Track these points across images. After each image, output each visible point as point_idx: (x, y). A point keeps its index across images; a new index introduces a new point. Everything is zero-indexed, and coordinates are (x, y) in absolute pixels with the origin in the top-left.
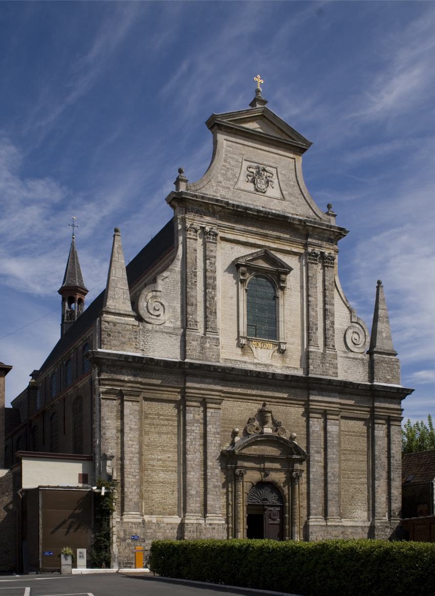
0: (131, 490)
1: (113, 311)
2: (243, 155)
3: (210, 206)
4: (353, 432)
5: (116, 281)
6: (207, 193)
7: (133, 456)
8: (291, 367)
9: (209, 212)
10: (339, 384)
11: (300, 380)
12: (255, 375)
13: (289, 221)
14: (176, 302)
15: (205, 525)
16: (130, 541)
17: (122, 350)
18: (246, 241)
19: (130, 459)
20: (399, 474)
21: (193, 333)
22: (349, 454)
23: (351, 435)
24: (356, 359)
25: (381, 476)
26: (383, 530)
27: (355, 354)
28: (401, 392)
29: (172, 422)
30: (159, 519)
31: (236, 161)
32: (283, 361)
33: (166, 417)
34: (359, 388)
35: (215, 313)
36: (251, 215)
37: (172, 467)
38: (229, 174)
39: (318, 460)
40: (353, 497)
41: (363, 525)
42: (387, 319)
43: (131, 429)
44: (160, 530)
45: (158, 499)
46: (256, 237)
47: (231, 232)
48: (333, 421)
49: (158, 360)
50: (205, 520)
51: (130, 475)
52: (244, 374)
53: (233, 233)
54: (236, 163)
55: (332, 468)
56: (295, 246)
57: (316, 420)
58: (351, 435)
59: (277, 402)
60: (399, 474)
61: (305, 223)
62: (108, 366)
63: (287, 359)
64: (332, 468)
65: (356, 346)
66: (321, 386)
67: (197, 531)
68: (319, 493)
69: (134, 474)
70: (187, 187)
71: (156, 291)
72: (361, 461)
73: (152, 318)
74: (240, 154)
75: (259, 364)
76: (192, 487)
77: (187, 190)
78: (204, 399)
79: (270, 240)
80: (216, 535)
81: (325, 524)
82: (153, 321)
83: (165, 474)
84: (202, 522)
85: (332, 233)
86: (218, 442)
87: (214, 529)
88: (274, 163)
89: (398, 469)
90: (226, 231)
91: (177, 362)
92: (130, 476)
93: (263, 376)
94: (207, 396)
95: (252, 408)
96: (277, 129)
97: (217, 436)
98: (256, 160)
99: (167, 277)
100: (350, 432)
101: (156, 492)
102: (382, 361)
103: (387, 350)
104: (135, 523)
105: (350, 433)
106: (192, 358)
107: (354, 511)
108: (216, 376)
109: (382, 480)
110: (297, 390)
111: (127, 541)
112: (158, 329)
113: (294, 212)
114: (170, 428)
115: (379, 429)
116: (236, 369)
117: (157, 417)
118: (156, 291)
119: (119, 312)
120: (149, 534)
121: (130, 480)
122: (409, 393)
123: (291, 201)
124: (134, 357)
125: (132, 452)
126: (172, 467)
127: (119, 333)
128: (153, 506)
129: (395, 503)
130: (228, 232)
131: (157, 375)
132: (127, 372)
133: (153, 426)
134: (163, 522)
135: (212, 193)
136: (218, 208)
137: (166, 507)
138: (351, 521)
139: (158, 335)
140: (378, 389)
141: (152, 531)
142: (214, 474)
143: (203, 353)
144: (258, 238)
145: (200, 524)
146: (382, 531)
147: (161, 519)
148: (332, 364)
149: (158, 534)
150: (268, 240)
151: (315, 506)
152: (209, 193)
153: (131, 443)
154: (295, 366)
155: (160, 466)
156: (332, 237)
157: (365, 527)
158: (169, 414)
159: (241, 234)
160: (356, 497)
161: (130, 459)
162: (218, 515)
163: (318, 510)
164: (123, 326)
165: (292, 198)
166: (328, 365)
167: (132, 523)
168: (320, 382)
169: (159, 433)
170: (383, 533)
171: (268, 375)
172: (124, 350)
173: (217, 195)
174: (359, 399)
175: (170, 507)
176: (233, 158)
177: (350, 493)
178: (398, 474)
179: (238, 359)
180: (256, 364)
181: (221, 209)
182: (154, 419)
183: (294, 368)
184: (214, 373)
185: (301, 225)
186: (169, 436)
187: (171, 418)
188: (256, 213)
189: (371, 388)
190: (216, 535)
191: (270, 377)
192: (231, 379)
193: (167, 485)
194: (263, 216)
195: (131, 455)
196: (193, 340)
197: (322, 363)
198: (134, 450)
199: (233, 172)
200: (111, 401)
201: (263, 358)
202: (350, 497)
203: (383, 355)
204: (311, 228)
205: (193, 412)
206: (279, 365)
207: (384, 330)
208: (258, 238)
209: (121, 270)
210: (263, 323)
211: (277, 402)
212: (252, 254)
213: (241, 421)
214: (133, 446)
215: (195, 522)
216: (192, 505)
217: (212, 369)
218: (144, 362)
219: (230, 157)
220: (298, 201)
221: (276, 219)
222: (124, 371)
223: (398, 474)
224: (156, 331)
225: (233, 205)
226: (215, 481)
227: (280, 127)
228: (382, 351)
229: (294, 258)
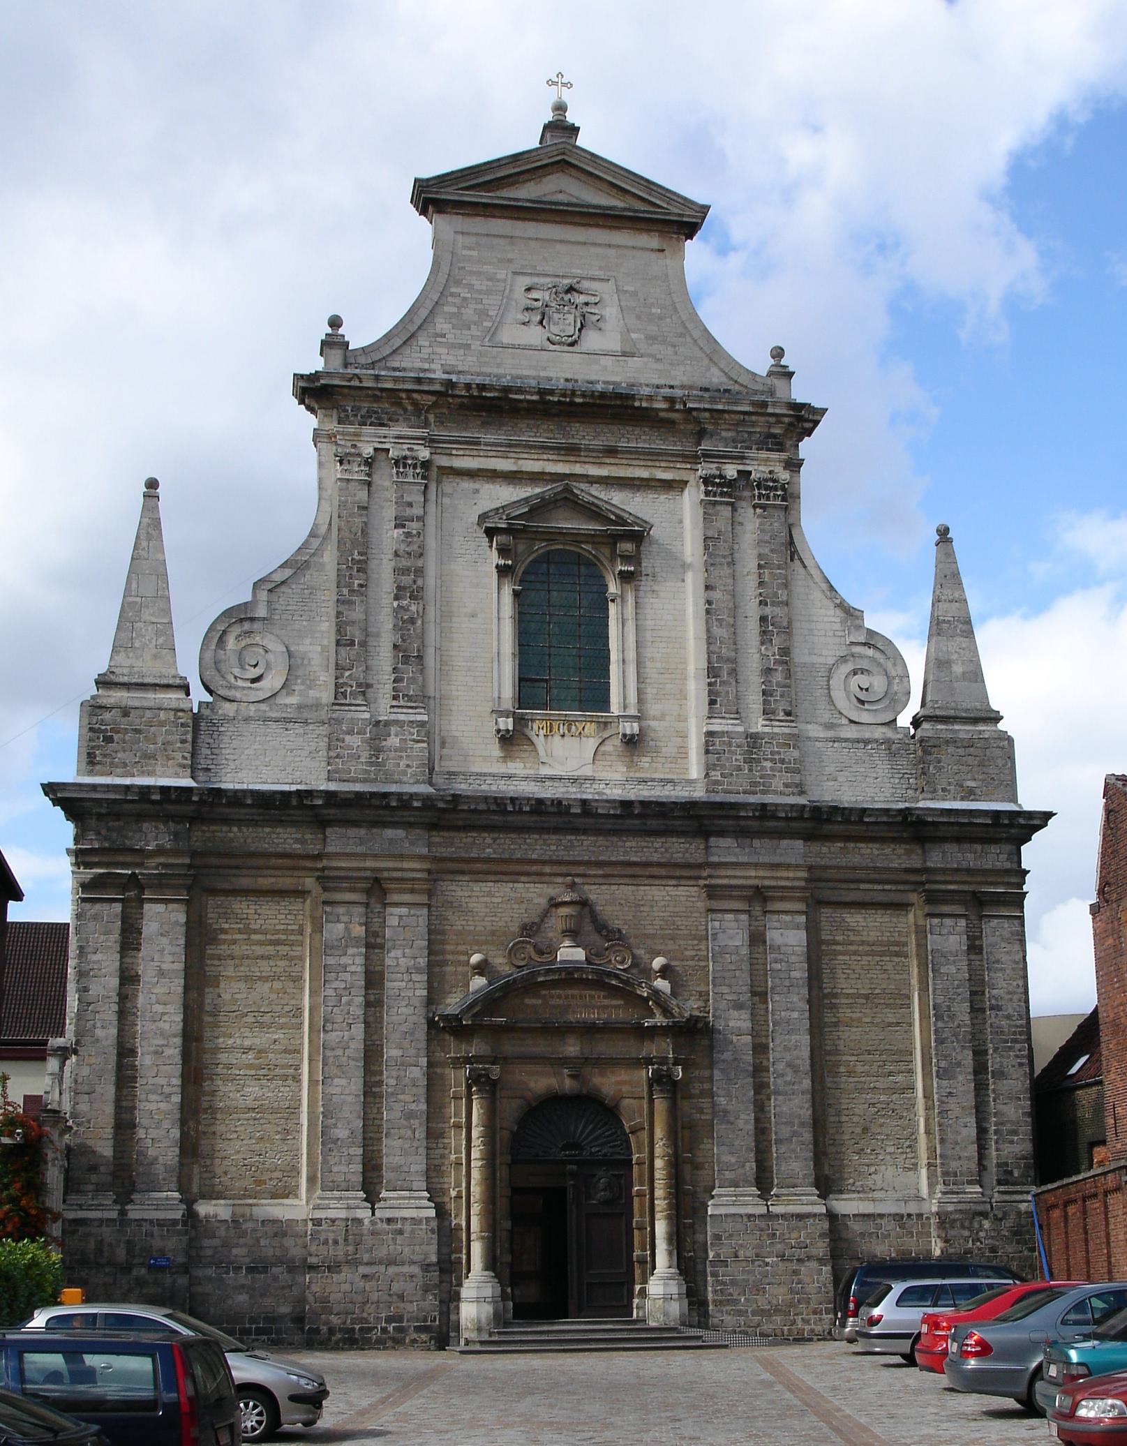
0: (153, 1133)
1: (126, 679)
2: (510, 261)
3: (404, 395)
4: (863, 943)
5: (137, 608)
6: (404, 365)
7: (165, 1042)
8: (653, 780)
9: (405, 410)
10: (794, 815)
11: (672, 810)
12: (528, 809)
13: (637, 404)
14: (308, 641)
15: (373, 1223)
16: (143, 1271)
17: (142, 773)
18: (514, 468)
19: (156, 1053)
20: (1023, 1056)
21: (349, 715)
22: (850, 1006)
23: (855, 953)
24: (866, 742)
25: (959, 1064)
26: (966, 1224)
27: (864, 727)
28: (1006, 822)
29: (287, 948)
30: (239, 1210)
31: (489, 280)
32: (631, 765)
33: (269, 937)
34: (867, 820)
35: (420, 658)
36: (525, 405)
37: (283, 1067)
38: (469, 313)
39: (739, 1029)
40: (865, 1130)
41: (903, 1211)
42: (964, 627)
43: (161, 973)
44: (241, 1241)
45: (240, 1156)
46: (545, 457)
47: (467, 452)
48: (787, 918)
49: (236, 791)
50: (373, 1209)
51: (155, 1093)
52: (493, 807)
53: (474, 453)
54: (490, 283)
55: (787, 1049)
56: (663, 464)
57: (730, 916)
58: (855, 953)
59: (604, 876)
60: (1023, 1056)
61: (685, 405)
62: (100, 816)
63: (644, 759)
64: (787, 1049)
65: (867, 706)
66: (742, 823)
67: (346, 1240)
68: (746, 1122)
69: (167, 1090)
70: (345, 357)
71: (252, 619)
72: (890, 1025)
73: (236, 688)
74: (500, 261)
75: (551, 778)
76: (337, 1119)
77: (346, 365)
78: (377, 880)
79: (587, 460)
80: (406, 1250)
81: (763, 1210)
82: (238, 695)
83: (262, 1087)
84: (364, 1214)
85: (772, 420)
86: (418, 993)
87: (401, 1232)
88: (601, 269)
89: (1015, 1041)
90: (454, 452)
91: (290, 792)
92: (153, 1097)
93: (551, 809)
94: (386, 874)
95: (530, 895)
96: (605, 187)
97: (416, 977)
98: (550, 270)
99: (283, 583)
100: (851, 943)
101: (235, 1136)
102: (947, 742)
103: (967, 710)
104: (160, 1223)
105: (851, 948)
106: (346, 776)
107: (872, 1169)
108: (412, 820)
109: (960, 1078)
110: (674, 840)
111: (135, 1272)
112: (252, 714)
113: (662, 382)
114: (281, 963)
115: (944, 931)
116: (468, 797)
117: (245, 936)
118: (252, 619)
119: (140, 681)
120: (209, 1252)
121: (153, 1107)
122: (1037, 822)
123: (653, 356)
124: (165, 790)
125: (162, 1034)
126: (283, 1067)
127: (138, 731)
128: (226, 1173)
129: (1012, 1142)
130: (461, 452)
131: (245, 830)
132: (157, 828)
133: (232, 962)
134: (251, 1218)
135: (418, 365)
136: (425, 397)
137: (265, 1177)
138: (860, 1199)
139: (253, 726)
140: (930, 819)
141: (216, 1242)
142: (407, 1081)
143: (378, 764)
144: (551, 457)
145: (359, 1221)
146: (963, 1227)
147: (247, 1210)
148: (782, 761)
149: (235, 1251)
150: (582, 459)
151: (733, 1160)
152: (409, 365)
153: (159, 1008)
154: (667, 776)
155: (250, 1066)
156: (776, 430)
157: (909, 1215)
158: (278, 927)
159: (499, 454)
160: (874, 1129)
161: (156, 1053)
162: (416, 1194)
163: (741, 1171)
164: (148, 714)
165: (656, 348)
166: (768, 764)
167: (151, 1221)
168: (732, 813)
169: (247, 979)
170: (966, 1233)
171: (569, 806)
172: (150, 774)
173: (433, 366)
174: (876, 852)
175: (276, 1175)
176: (479, 273)
177: (856, 1119)
178: (1017, 1056)
179: (490, 771)
180: (543, 780)
181: (434, 398)
182: (235, 942)
183: (661, 780)
184: (406, 813)
185: (677, 411)
186: (277, 985)
187: (284, 937)
188: (535, 398)
189: (905, 818)
190: (406, 1250)
191: (576, 810)
192: (460, 823)
193: (270, 1116)
194: (559, 402)
195: (161, 1042)
196: (350, 732)
197: (749, 761)
198: (167, 1026)
199: (481, 306)
200: (106, 906)
201: (570, 760)
202: (858, 1130)
203: (952, 724)
204: (707, 415)
205: (345, 919)
206: (617, 776)
207: (955, 657)
208: (551, 457)
209: (154, 577)
210: (561, 669)
211: (604, 876)
212: (526, 500)
213: (493, 933)
214: (165, 1018)
215: (343, 1214)
216: (335, 1169)
217: (394, 804)
218: (195, 798)
219: (471, 273)
220: (676, 353)
221: (599, 406)
222: (145, 825)
223: (1017, 1056)
224: (247, 719)
225: (468, 386)
226: (408, 1098)
227: (614, 181)
228: (952, 713)
229: (663, 497)
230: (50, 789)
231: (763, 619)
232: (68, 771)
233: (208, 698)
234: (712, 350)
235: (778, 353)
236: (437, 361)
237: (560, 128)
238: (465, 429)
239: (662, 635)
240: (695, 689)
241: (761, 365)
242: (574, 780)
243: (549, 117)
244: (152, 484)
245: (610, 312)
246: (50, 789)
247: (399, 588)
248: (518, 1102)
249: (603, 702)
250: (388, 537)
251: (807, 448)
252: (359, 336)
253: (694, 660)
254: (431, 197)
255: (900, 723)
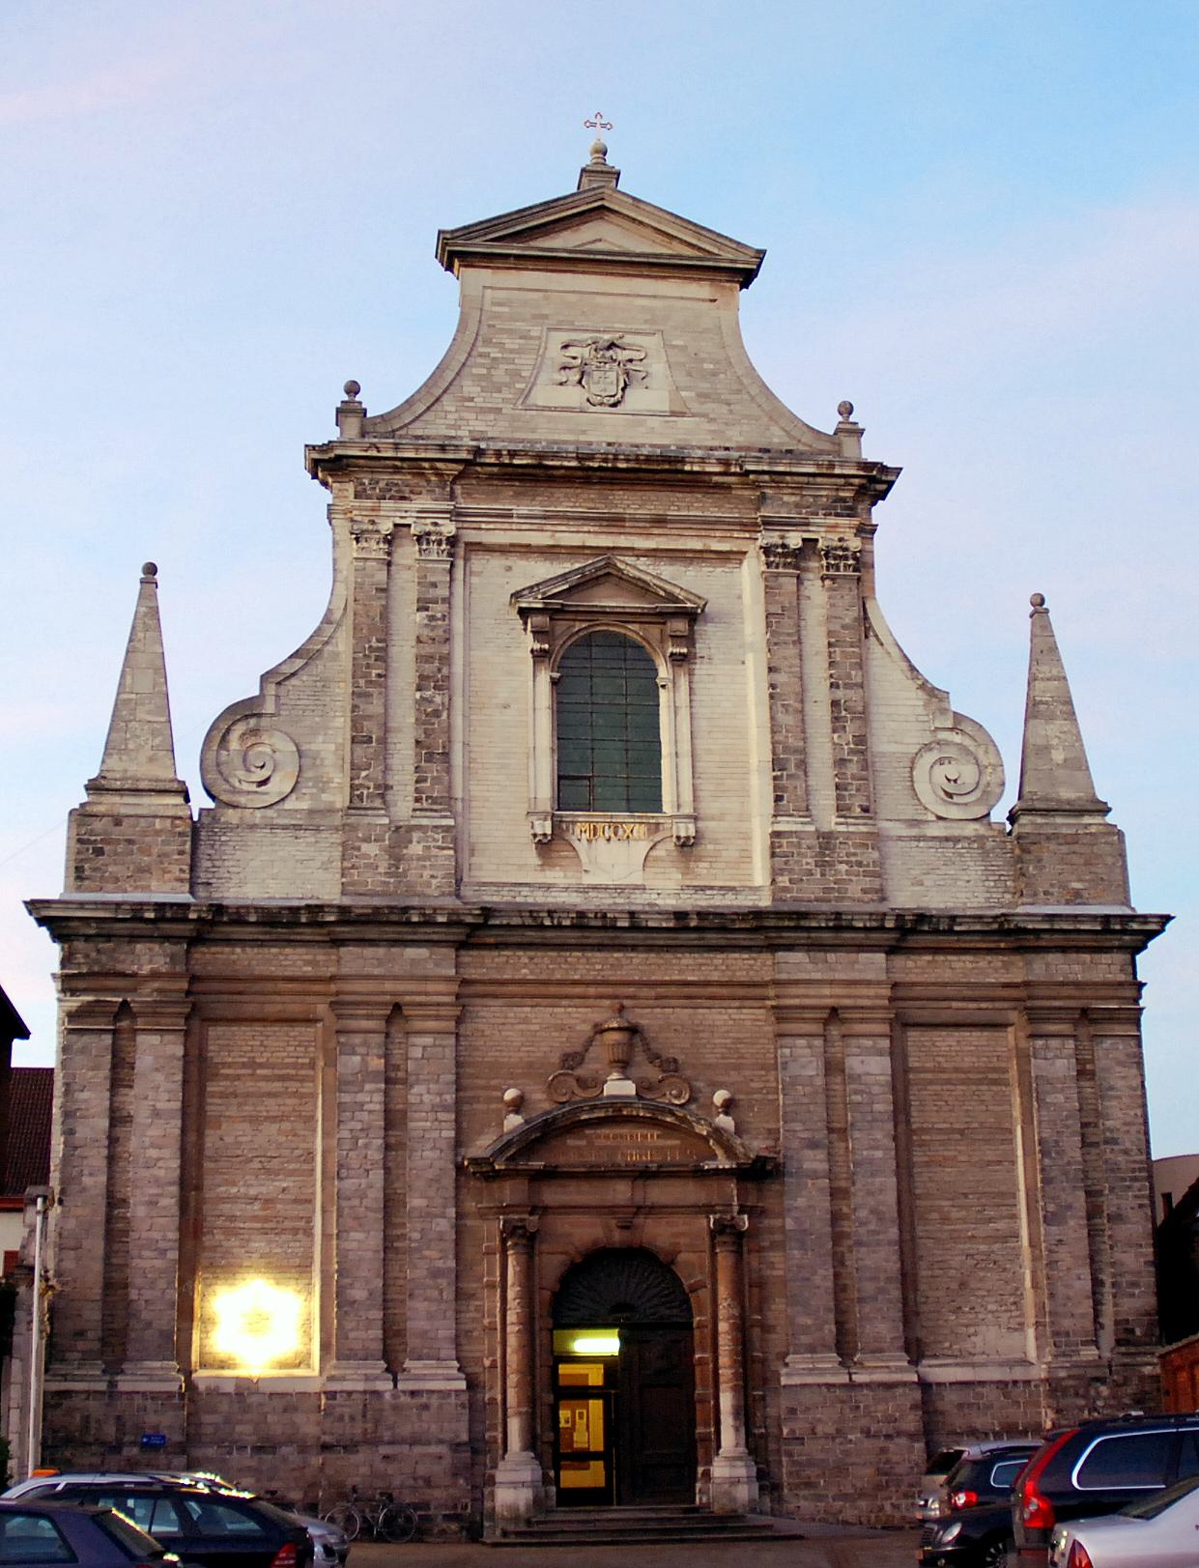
0: (148, 1294)
2: (546, 317)
4: (957, 1070)
6: (427, 432)
8: (711, 888)
9: (429, 481)
13: (687, 468)
14: (320, 739)
15: (395, 1396)
16: (135, 1450)
21: (367, 820)
22: (943, 1143)
23: (948, 1082)
24: (956, 840)
32: (686, 872)
35: (446, 755)
38: (500, 375)
40: (963, 1285)
43: (156, 1113)
44: (248, 1416)
48: (868, 1043)
50: (395, 1381)
51: (149, 1248)
52: (529, 921)
55: (870, 1193)
57: (802, 1042)
58: (948, 1082)
63: (702, 865)
64: (870, 1193)
69: (162, 1245)
71: (259, 715)
72: (989, 1163)
73: (241, 792)
74: (535, 317)
75: (595, 888)
80: (433, 1427)
81: (845, 1379)
82: (243, 800)
83: (270, 1242)
86: (444, 1134)
87: (426, 1407)
89: (1135, 1179)
92: (146, 1253)
93: (593, 923)
94: (408, 998)
97: (442, 1116)
98: (589, 325)
99: (293, 674)
100: (943, 1071)
102: (1049, 838)
104: (154, 1396)
106: (362, 890)
107: (972, 1330)
109: (1072, 1223)
111: (126, 1451)
113: (715, 443)
114: (291, 1102)
115: (1050, 1055)
120: (209, 1430)
125: (157, 1182)
127: (130, 842)
133: (234, 1101)
139: (259, 834)
142: (432, 1236)
146: (1077, 1394)
148: (860, 864)
149: (239, 1428)
153: (153, 1153)
155: (255, 1219)
157: (1015, 1382)
164: (143, 822)
166: (844, 867)
167: (144, 1394)
169: (254, 1120)
170: (1082, 1402)
172: (146, 889)
176: (510, 332)
177: (952, 1272)
181: (461, 467)
182: (238, 1077)
183: (721, 888)
185: (734, 474)
186: (286, 1126)
188: (574, 464)
191: (624, 923)
192: (492, 940)
194: (600, 469)
196: (367, 840)
198: (162, 1173)
201: (617, 865)
202: (954, 1286)
204: (766, 477)
205: (362, 1050)
207: (1055, 742)
212: (564, 576)
215: (360, 1386)
216: (352, 1335)
217: (415, 919)
218: (193, 916)
219: (503, 331)
222: (139, 946)
224: (253, 827)
225: (498, 453)
230: (32, 906)
231: (835, 704)
232: (53, 885)
233: (210, 804)
234: (776, 411)
235: (847, 409)
236: (463, 425)
237: (600, 172)
238: (496, 501)
239: (718, 717)
240: (760, 785)
241: (827, 422)
242: (620, 889)
243: (587, 160)
244: (151, 569)
245: (657, 367)
246: (32, 906)
247: (422, 677)
248: (562, 1258)
249: (654, 803)
250: (408, 622)
251: (880, 512)
252: (376, 403)
253: (758, 751)
254: (458, 251)
255: (994, 818)
